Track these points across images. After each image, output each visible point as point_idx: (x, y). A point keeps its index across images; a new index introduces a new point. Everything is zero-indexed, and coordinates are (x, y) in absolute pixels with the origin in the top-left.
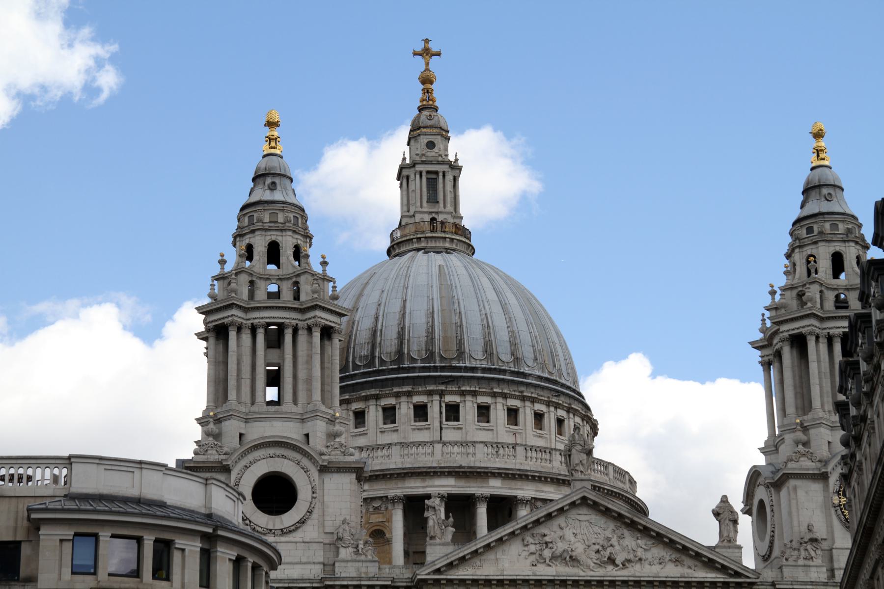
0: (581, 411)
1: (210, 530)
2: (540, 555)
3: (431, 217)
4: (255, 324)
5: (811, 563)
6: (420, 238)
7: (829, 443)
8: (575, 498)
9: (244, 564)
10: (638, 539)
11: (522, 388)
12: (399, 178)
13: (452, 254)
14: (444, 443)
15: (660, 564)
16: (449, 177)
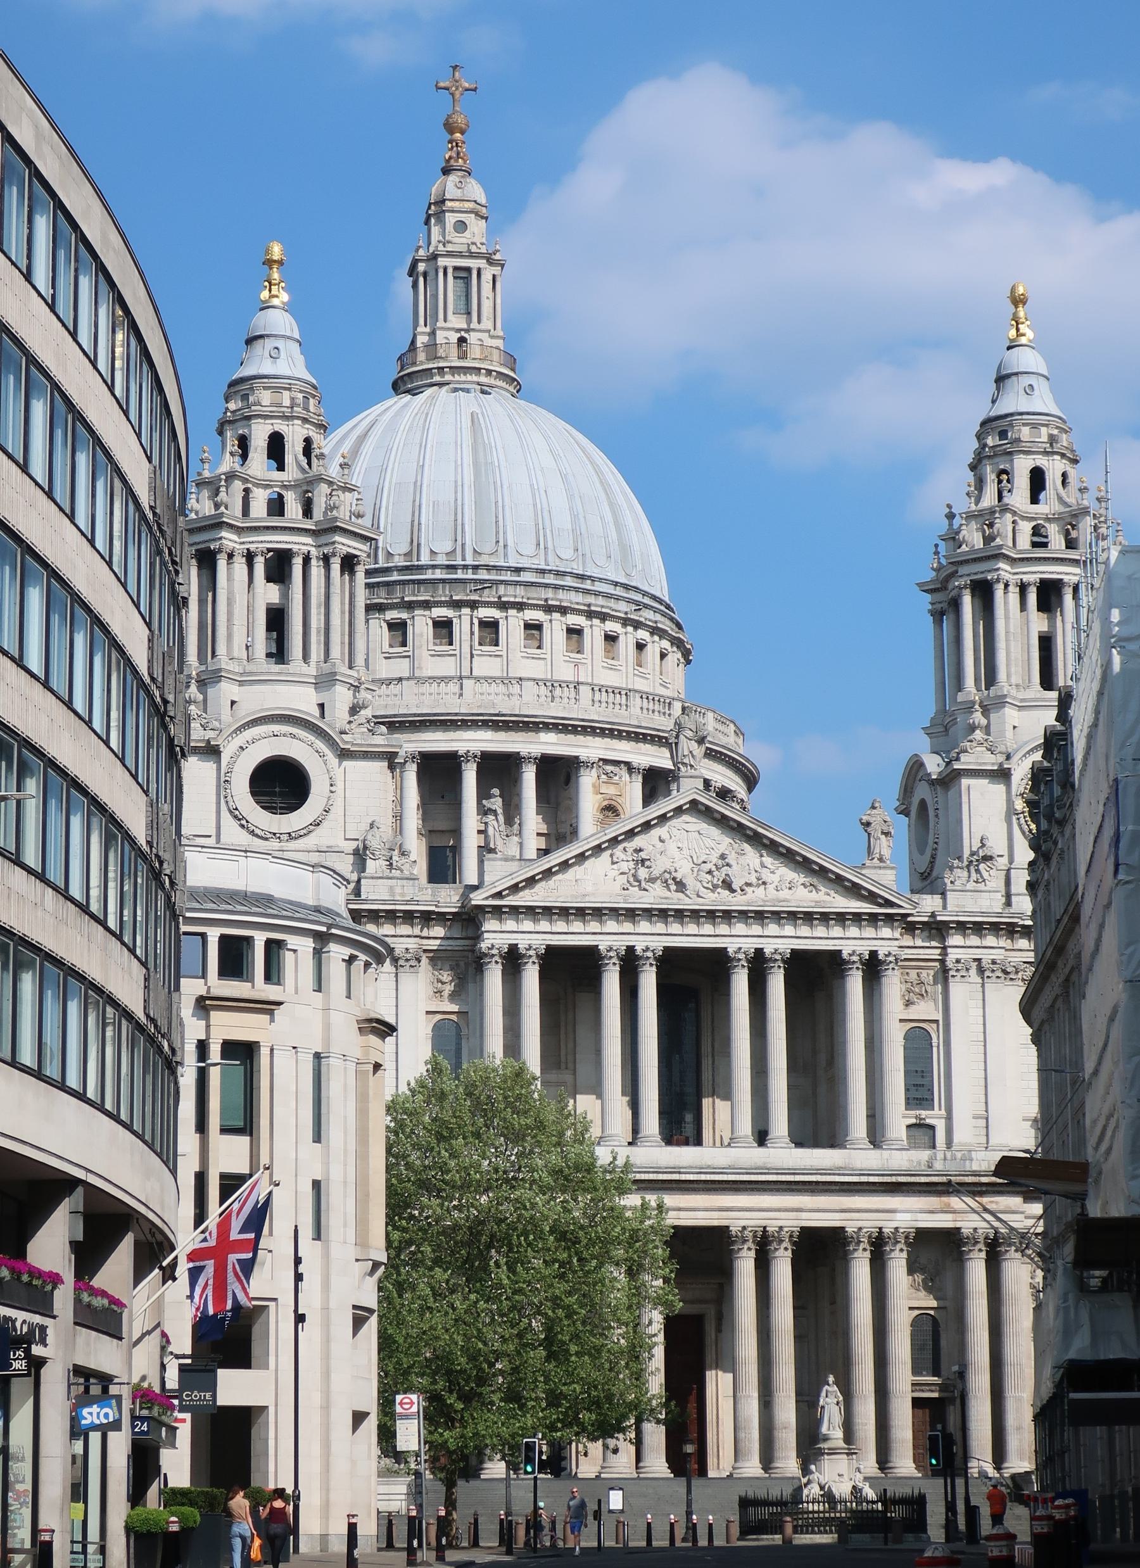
0: (670, 632)
1: (324, 929)
2: (634, 876)
3: (458, 335)
4: (252, 550)
5: (981, 886)
6: (443, 368)
7: (1015, 727)
8: (682, 802)
9: (356, 963)
10: (762, 856)
11: (591, 599)
12: (412, 271)
13: (490, 394)
14: (478, 679)
15: (790, 888)
16: (487, 276)
